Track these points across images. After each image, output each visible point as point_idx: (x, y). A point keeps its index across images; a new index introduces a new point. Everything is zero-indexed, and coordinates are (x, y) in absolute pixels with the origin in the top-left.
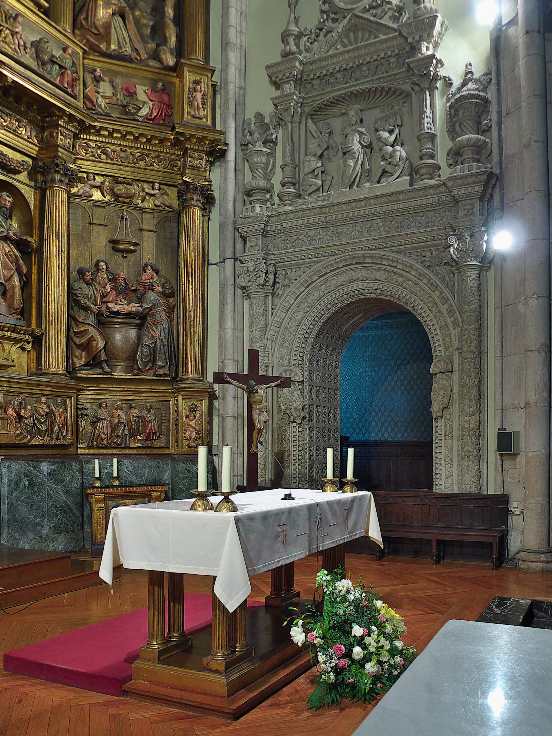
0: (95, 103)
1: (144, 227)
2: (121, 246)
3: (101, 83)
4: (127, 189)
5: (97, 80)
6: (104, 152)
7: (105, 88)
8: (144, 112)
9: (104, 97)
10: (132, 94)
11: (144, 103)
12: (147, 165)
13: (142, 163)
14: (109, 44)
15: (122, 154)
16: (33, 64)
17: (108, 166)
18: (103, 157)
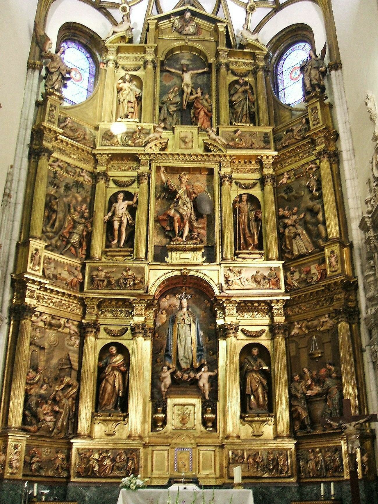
0: (292, 285)
1: (325, 341)
2: (316, 356)
3: (295, 274)
4: (313, 323)
5: (292, 273)
6: (300, 309)
7: (297, 276)
8: (315, 278)
9: (296, 280)
10: (308, 272)
11: (315, 274)
12: (320, 306)
13: (318, 306)
14: (292, 253)
15: (308, 306)
16: (254, 285)
17: (303, 315)
18: (300, 311)
